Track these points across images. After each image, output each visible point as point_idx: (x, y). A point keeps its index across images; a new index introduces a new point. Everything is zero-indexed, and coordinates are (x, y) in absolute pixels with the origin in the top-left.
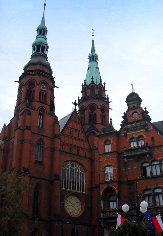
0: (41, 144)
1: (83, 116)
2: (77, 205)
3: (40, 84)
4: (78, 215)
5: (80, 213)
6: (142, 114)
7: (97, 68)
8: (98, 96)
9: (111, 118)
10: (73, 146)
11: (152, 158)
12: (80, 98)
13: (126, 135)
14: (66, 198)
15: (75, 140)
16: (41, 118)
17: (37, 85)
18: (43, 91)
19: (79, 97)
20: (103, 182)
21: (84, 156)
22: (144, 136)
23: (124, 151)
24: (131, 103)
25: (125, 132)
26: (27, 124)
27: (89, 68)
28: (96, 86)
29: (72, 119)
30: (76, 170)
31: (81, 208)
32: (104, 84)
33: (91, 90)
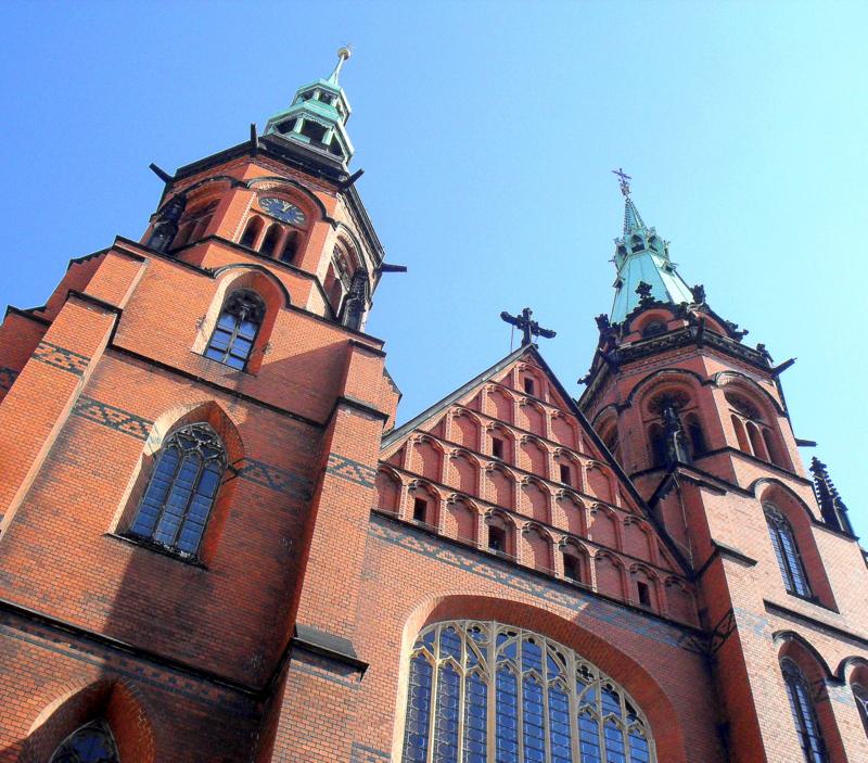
27: (619, 285)
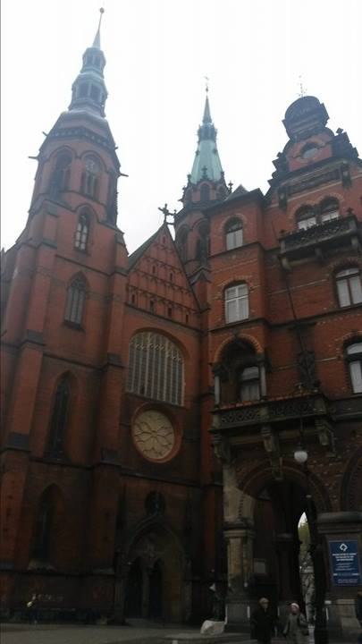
2: (163, 433)
4: (165, 458)
5: (170, 454)
6: (329, 147)
7: (215, 151)
10: (158, 299)
13: (283, 204)
17: (77, 157)
21: (184, 321)
22: (340, 197)
23: (280, 240)
24: (297, 124)
30: (163, 352)
31: (172, 442)
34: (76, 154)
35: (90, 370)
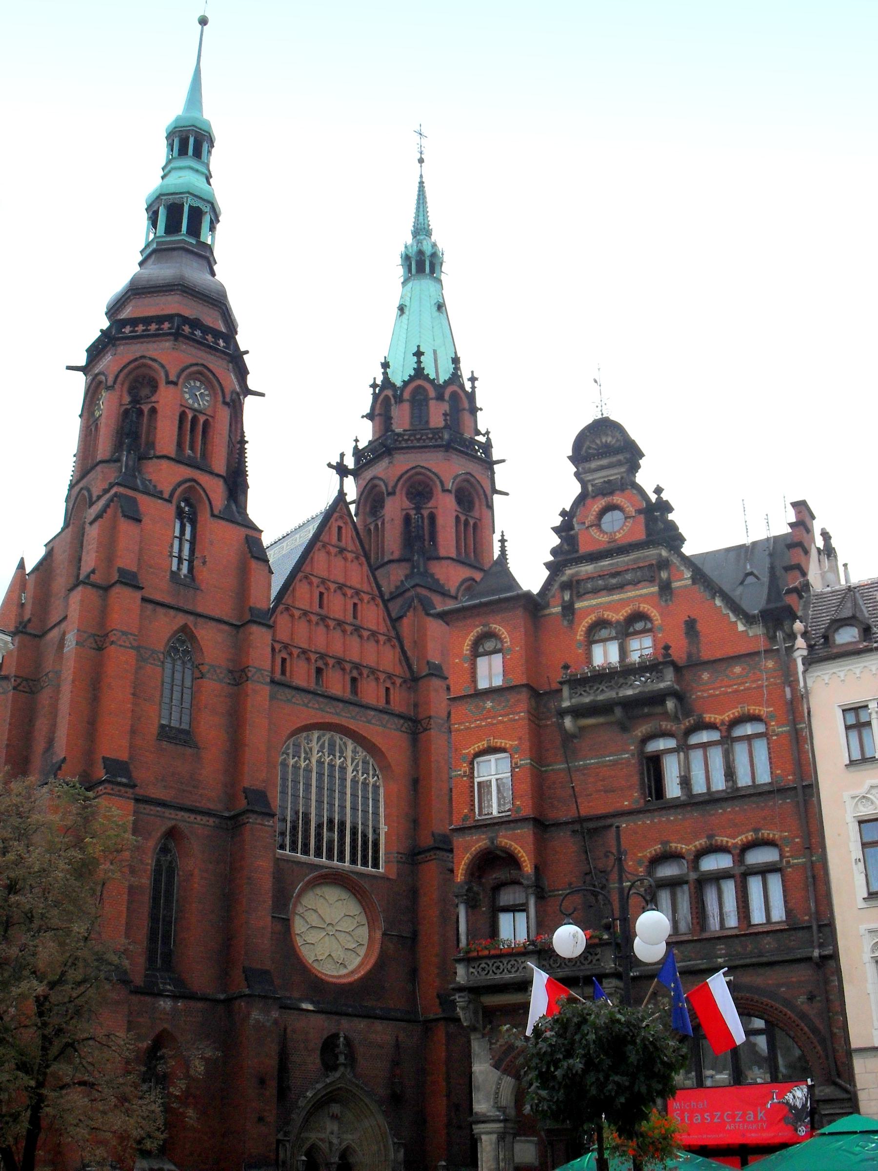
0: (186, 652)
1: (377, 525)
2: (348, 925)
3: (181, 380)
4: (352, 972)
7: (440, 307)
8: (446, 436)
9: (503, 536)
10: (331, 661)
11: (688, 713)
12: (361, 446)
13: (568, 609)
14: (300, 895)
15: (338, 634)
16: (188, 536)
17: (169, 382)
18: (195, 410)
19: (356, 441)
20: (468, 824)
21: (382, 704)
22: (654, 614)
23: (561, 683)
24: (594, 465)
25: (567, 597)
26: (121, 563)
27: (401, 309)
28: (435, 390)
29: (324, 537)
30: (343, 769)
31: (365, 941)
32: (473, 379)
33: (412, 408)
34: (167, 376)
35: (211, 821)
